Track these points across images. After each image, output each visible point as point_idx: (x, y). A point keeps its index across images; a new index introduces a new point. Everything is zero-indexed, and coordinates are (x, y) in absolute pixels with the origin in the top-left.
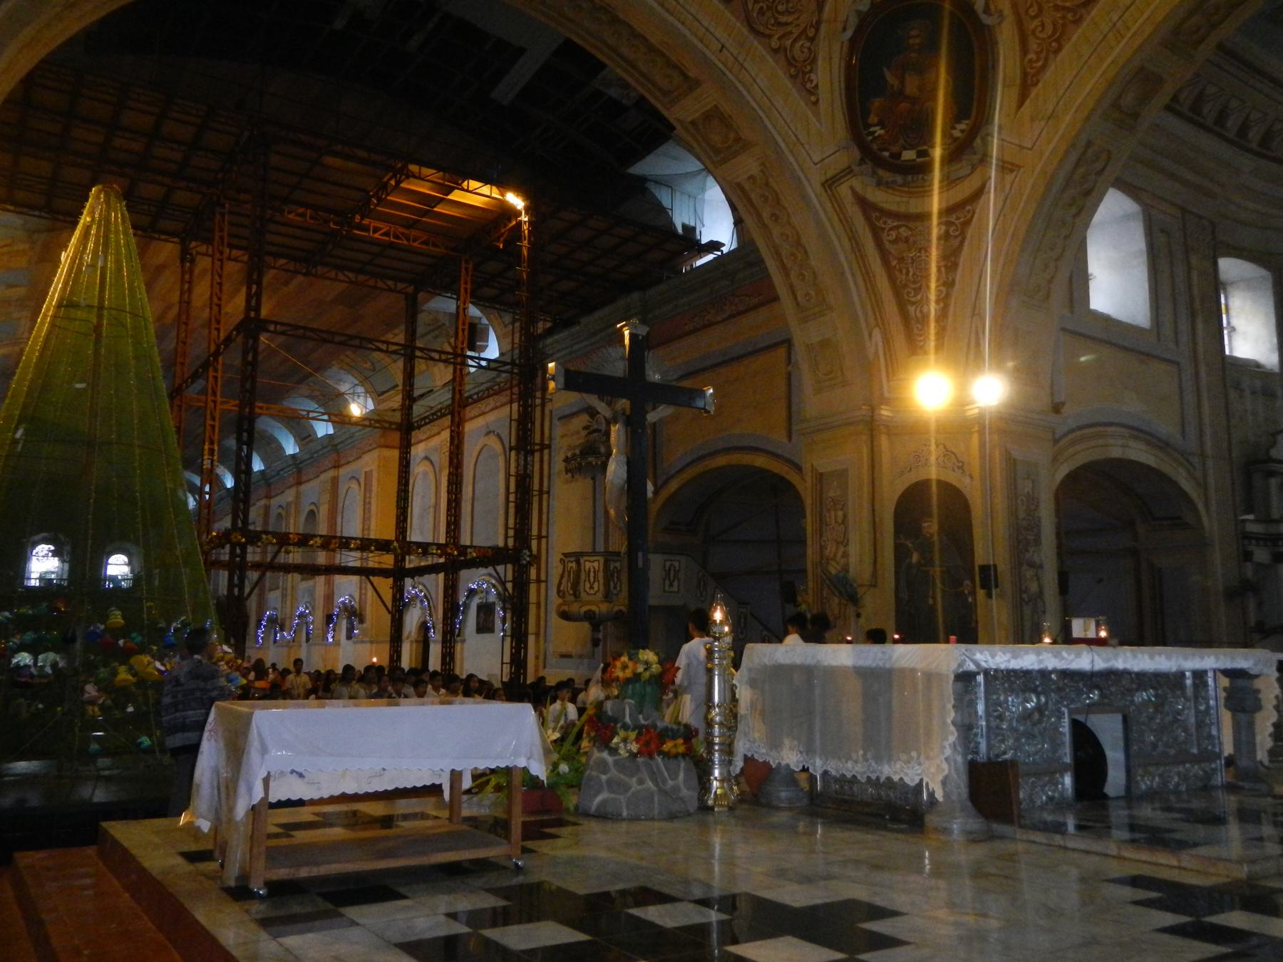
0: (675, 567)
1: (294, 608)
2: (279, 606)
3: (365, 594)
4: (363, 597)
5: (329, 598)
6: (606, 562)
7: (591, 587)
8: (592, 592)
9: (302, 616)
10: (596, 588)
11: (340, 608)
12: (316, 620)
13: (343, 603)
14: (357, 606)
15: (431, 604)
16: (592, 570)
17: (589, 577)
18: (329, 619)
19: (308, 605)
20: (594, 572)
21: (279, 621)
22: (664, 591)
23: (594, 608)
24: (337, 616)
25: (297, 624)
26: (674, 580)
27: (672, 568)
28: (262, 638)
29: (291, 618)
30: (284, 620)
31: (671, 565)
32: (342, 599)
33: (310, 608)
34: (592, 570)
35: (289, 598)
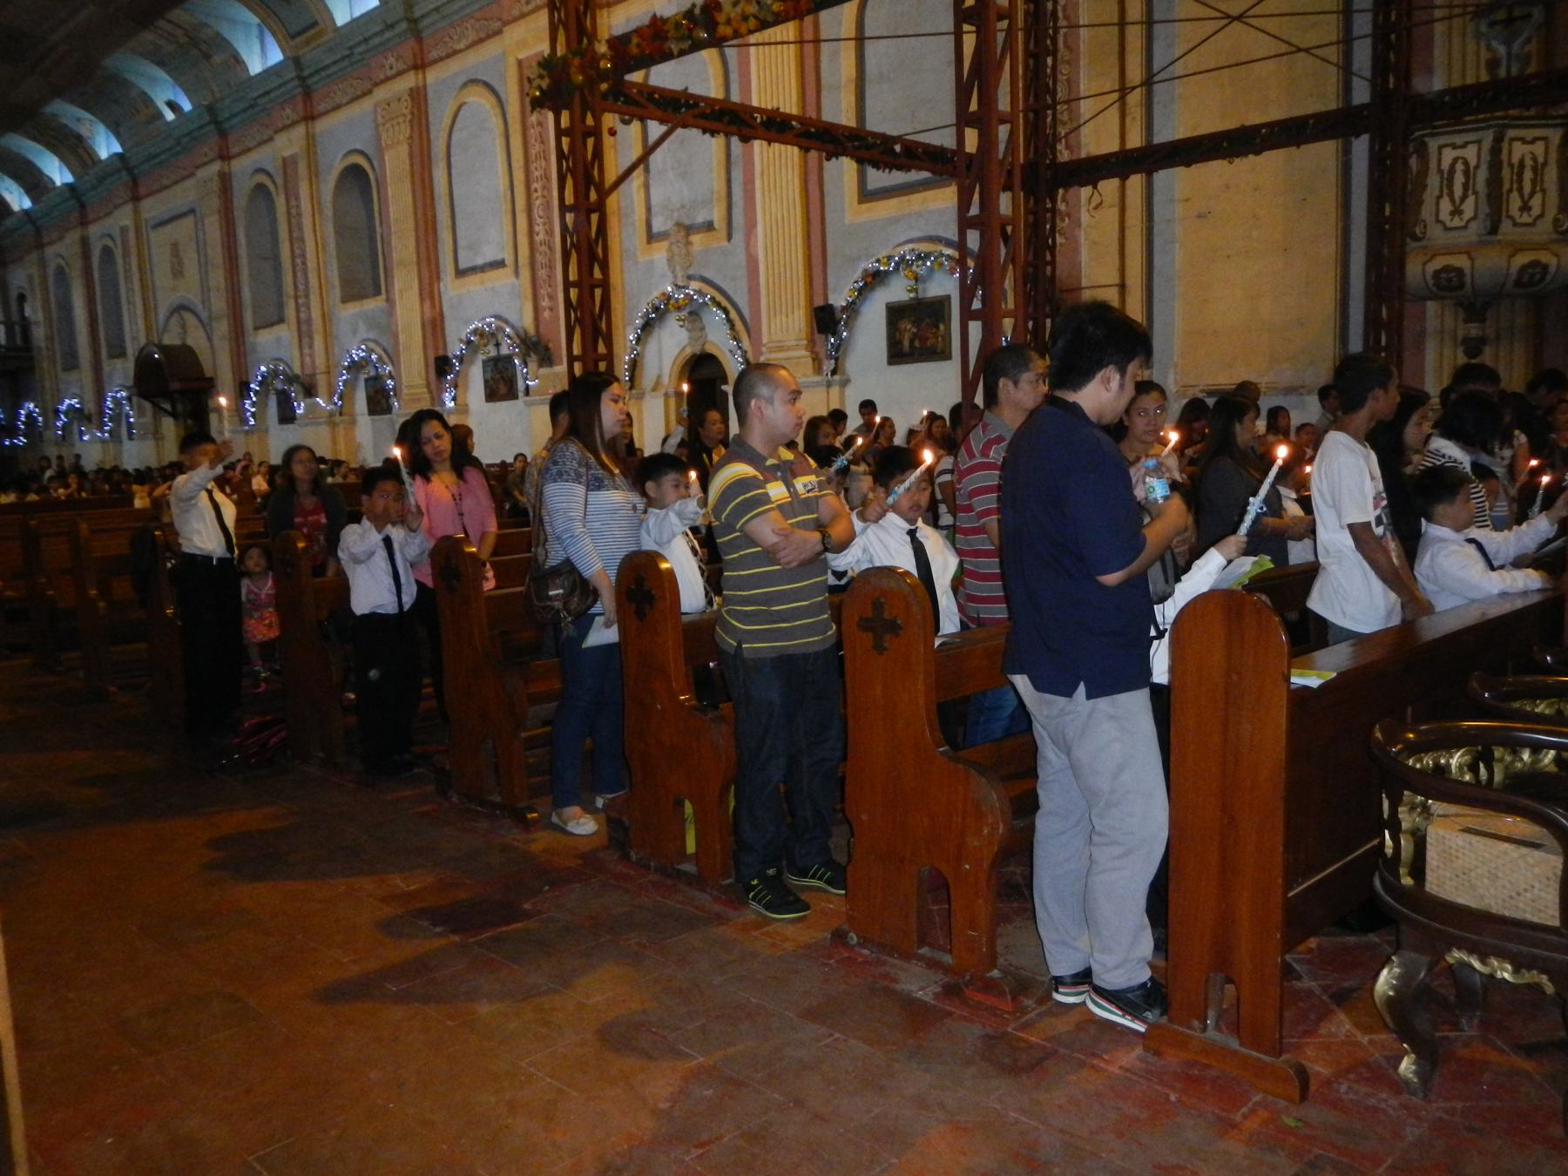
7: (1525, 208)
8: (1526, 219)
10: (1536, 211)
16: (1529, 162)
17: (1520, 181)
20: (1534, 169)
34: (1529, 162)
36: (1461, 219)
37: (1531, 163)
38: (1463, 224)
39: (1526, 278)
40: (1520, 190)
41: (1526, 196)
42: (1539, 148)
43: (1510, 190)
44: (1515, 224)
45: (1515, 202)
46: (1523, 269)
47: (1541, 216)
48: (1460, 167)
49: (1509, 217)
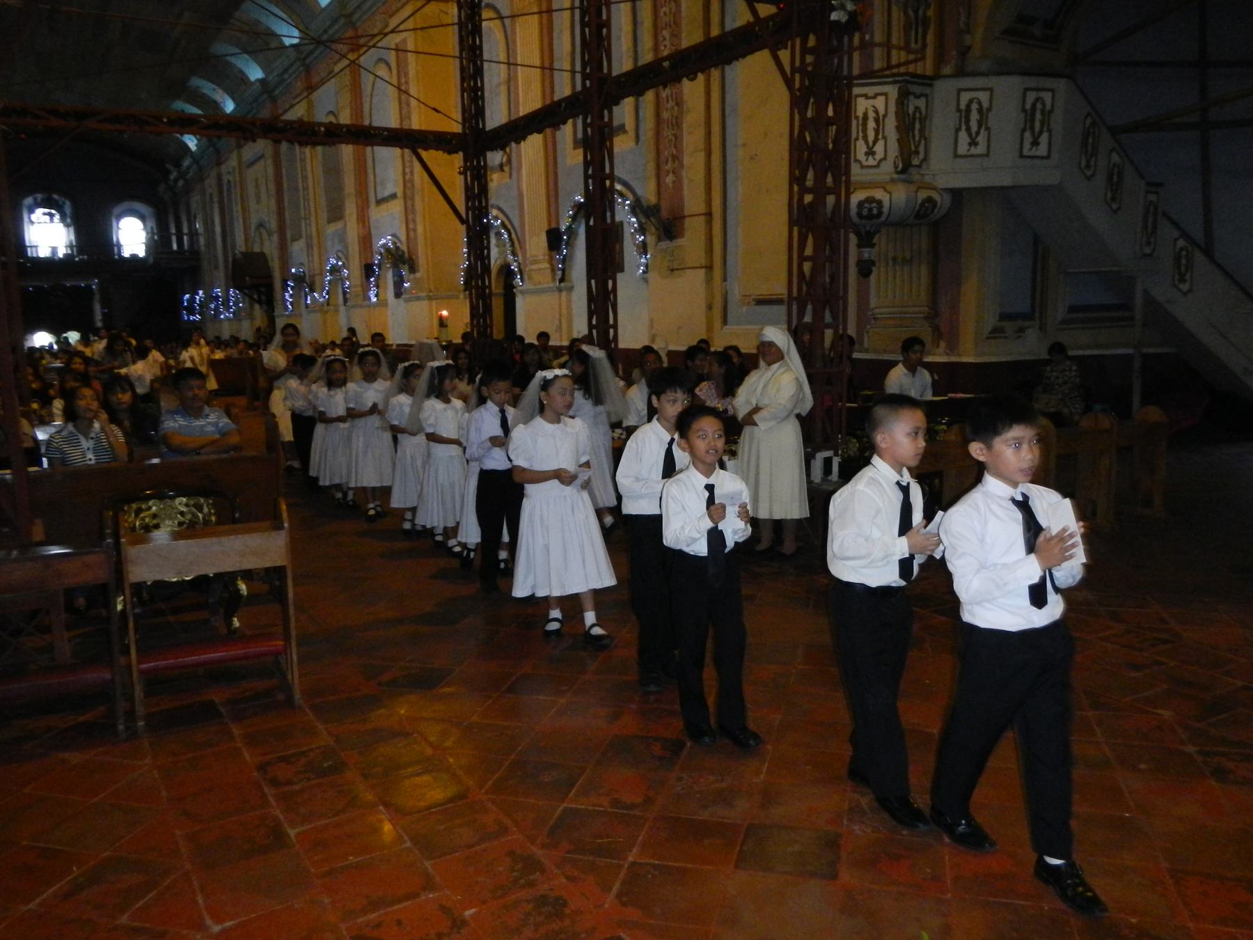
0: (1044, 104)
1: (323, 260)
2: (304, 259)
3: (415, 230)
4: (412, 234)
5: (366, 241)
6: (904, 96)
7: (870, 152)
8: (871, 162)
9: (335, 270)
10: (879, 155)
11: (381, 254)
12: (352, 275)
13: (384, 246)
14: (404, 248)
15: (514, 236)
18: (368, 270)
19: (340, 255)
20: (877, 120)
21: (307, 279)
22: (1022, 156)
23: (879, 194)
24: (379, 266)
25: (330, 282)
26: (1041, 133)
27: (1039, 106)
28: (292, 303)
29: (322, 274)
30: (312, 276)
31: (1037, 99)
32: (383, 241)
33: (344, 260)
35: (316, 249)
36: (875, 159)
37: (874, 115)
38: (875, 163)
39: (865, 212)
40: (865, 138)
41: (871, 144)
42: (880, 103)
43: (857, 139)
44: (862, 167)
45: (861, 148)
46: (861, 204)
47: (885, 158)
48: (975, 106)
49: (857, 161)
